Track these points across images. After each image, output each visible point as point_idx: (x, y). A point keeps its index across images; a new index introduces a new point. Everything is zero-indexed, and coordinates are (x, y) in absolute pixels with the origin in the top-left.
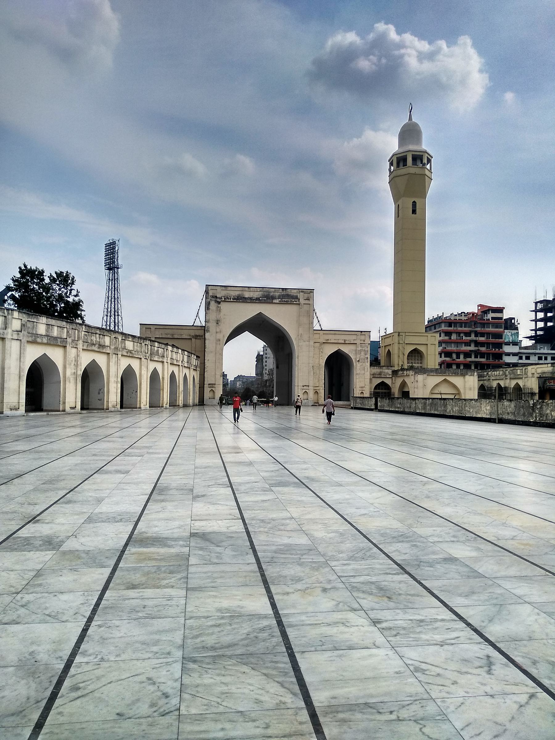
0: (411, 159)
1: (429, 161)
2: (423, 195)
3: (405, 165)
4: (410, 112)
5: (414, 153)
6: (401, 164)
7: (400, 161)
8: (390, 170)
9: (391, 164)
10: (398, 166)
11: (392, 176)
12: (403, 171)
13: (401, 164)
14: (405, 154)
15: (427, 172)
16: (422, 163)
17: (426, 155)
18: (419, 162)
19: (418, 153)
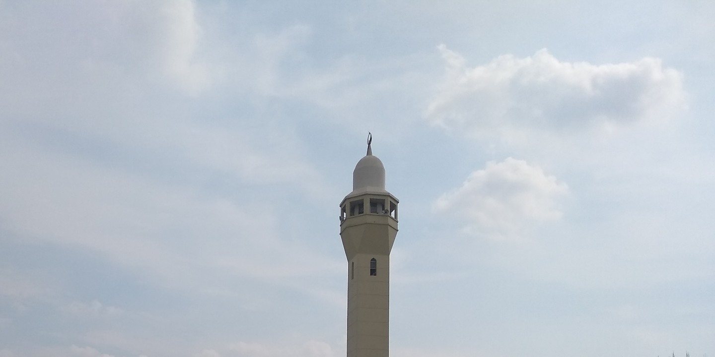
0: (369, 204)
1: (394, 207)
2: (386, 250)
3: (361, 212)
4: (369, 144)
5: (372, 197)
6: (357, 211)
7: (352, 207)
8: (341, 218)
9: (343, 210)
10: (352, 212)
11: (344, 226)
12: (358, 219)
13: (357, 211)
14: (360, 198)
15: (391, 222)
16: (383, 209)
17: (390, 199)
18: (379, 208)
19: (378, 198)
